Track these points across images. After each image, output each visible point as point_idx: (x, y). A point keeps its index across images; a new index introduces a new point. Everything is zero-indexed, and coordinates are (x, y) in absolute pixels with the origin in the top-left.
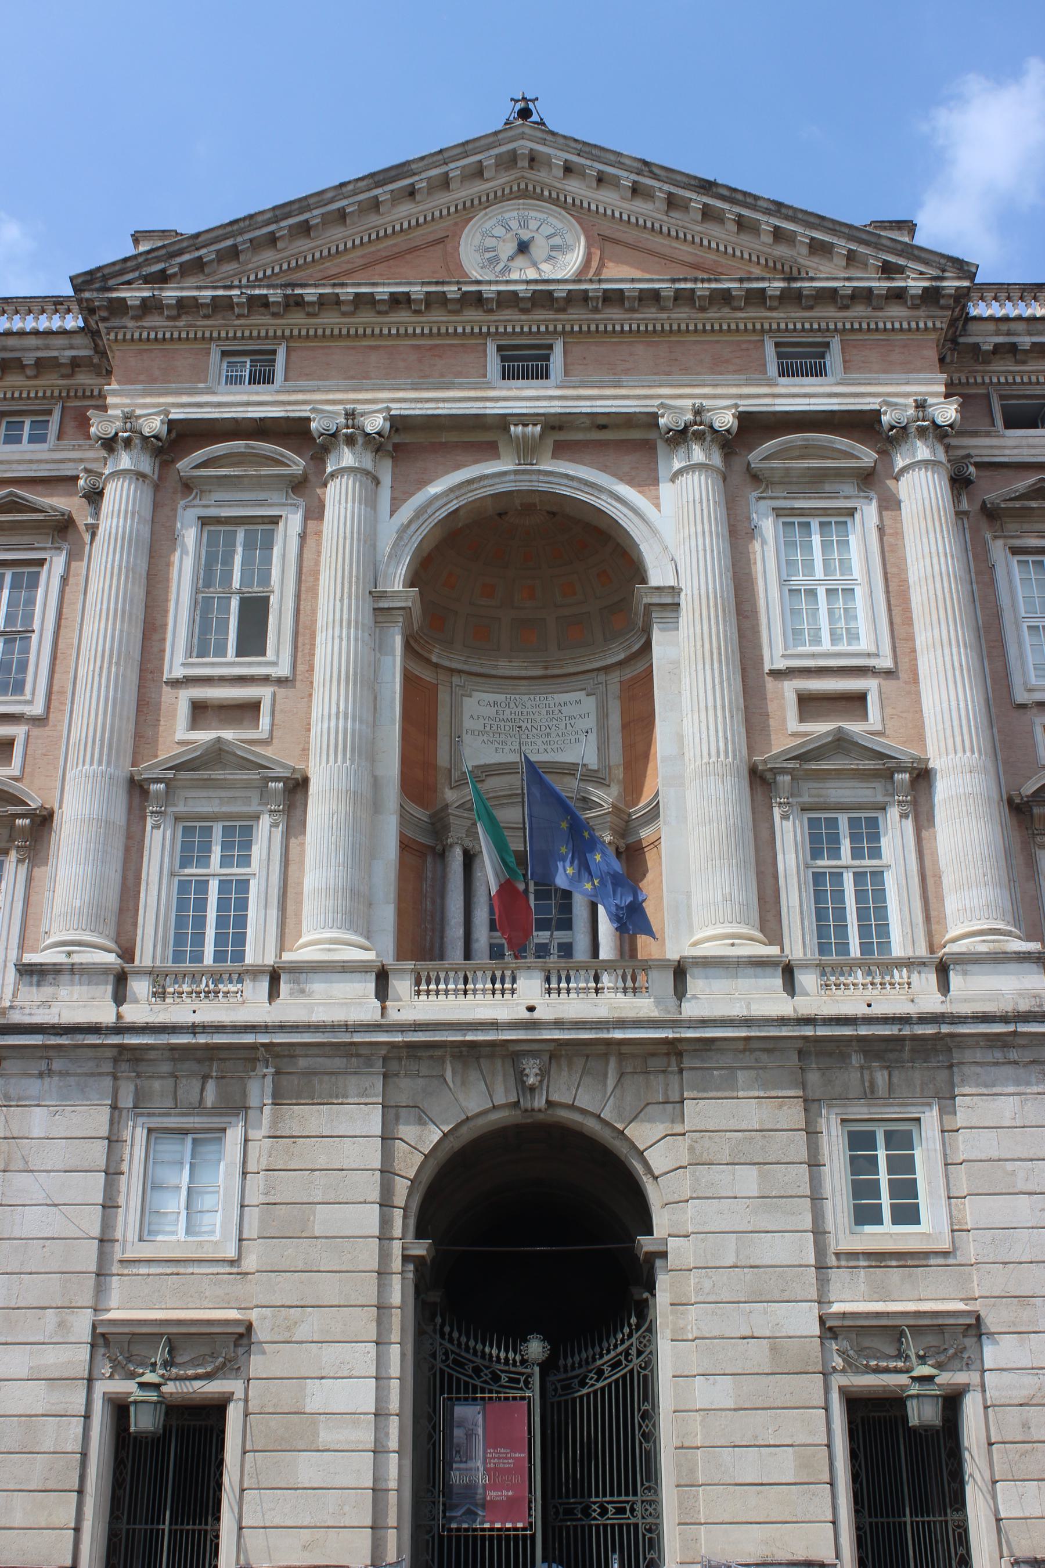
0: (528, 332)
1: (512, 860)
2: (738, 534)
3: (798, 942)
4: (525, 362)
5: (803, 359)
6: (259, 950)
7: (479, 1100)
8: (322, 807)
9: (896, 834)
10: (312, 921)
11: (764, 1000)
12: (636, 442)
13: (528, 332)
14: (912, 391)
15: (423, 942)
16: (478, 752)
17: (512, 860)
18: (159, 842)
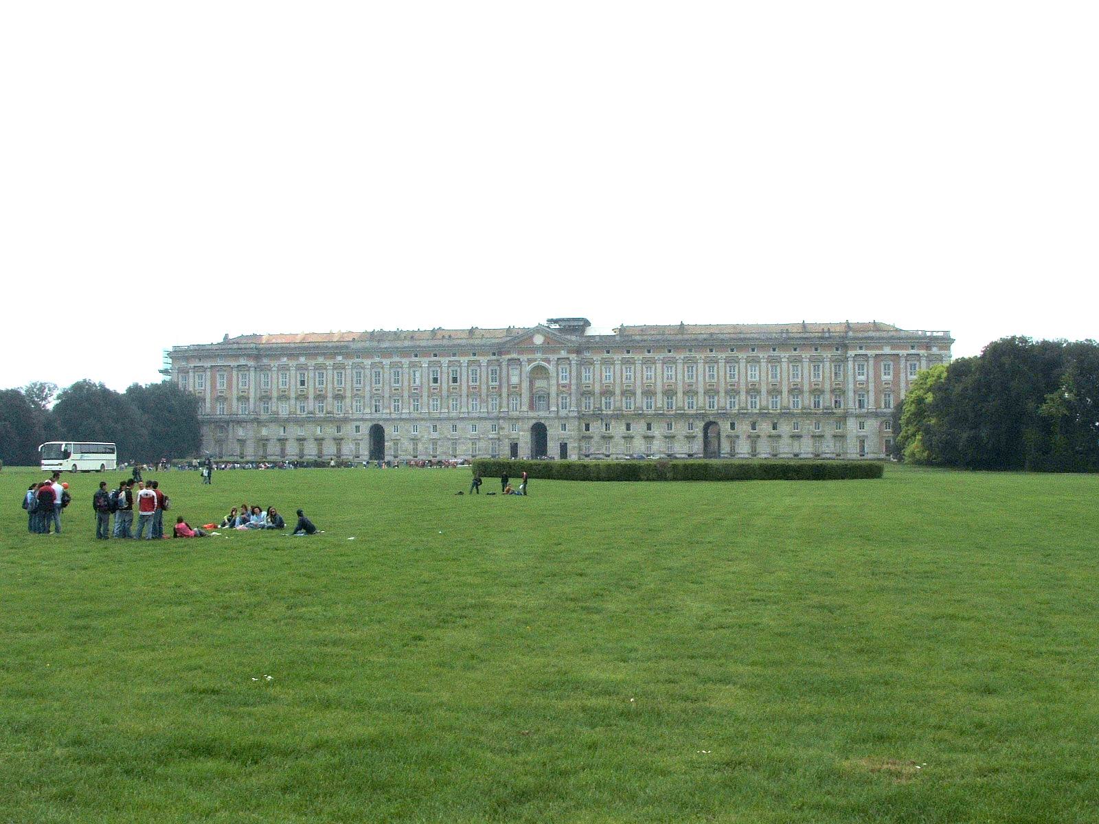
7: (534, 421)
12: (548, 361)
17: (537, 399)
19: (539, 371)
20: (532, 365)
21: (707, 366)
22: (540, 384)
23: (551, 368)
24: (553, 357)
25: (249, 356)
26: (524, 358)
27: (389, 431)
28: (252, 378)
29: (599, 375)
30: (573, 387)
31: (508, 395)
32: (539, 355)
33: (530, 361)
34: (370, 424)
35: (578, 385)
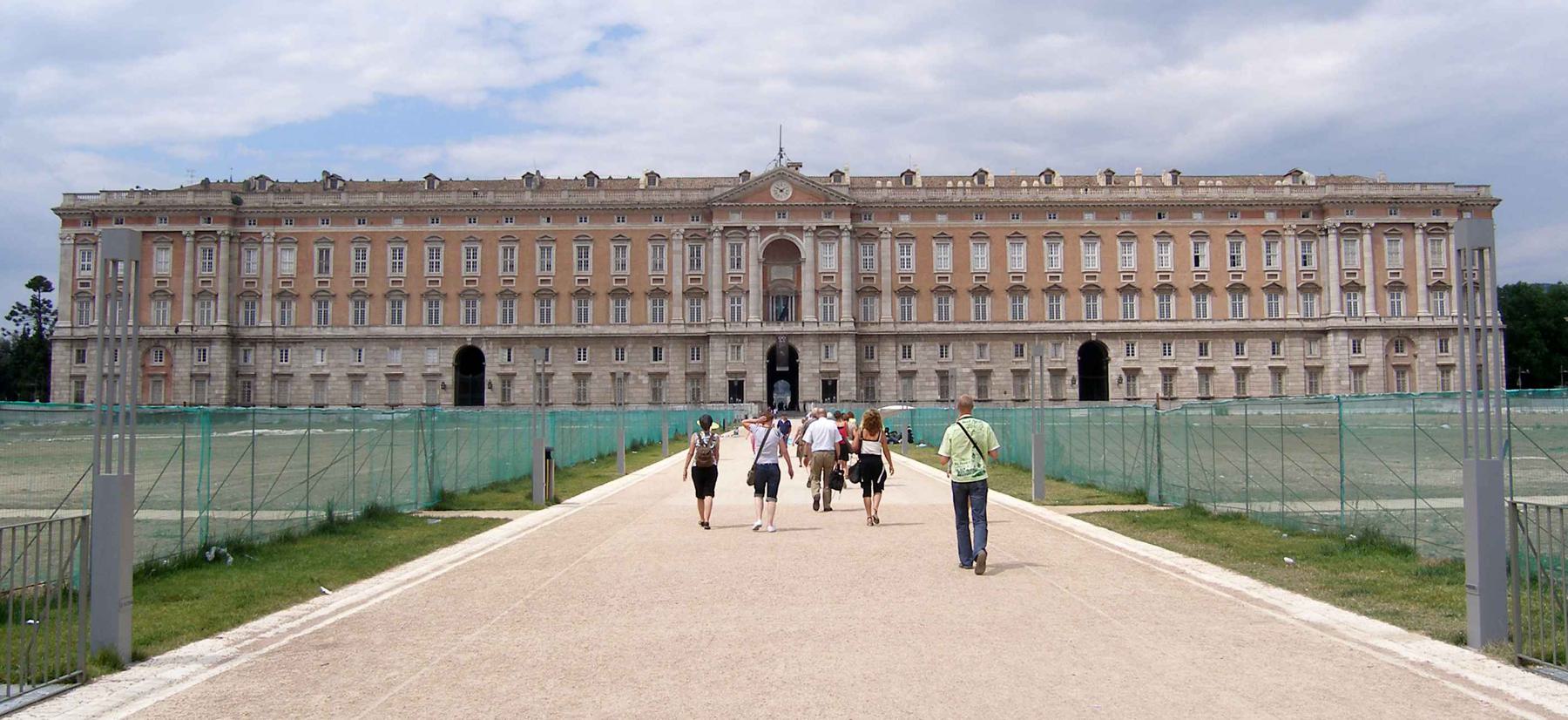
0: (782, 209)
1: (781, 304)
2: (816, 248)
3: (821, 318)
4: (782, 215)
5: (828, 214)
6: (743, 319)
8: (751, 297)
9: (836, 300)
10: (752, 317)
11: (815, 328)
12: (799, 230)
13: (782, 209)
14: (845, 223)
15: (766, 319)
16: (774, 277)
17: (781, 304)
18: (728, 300)
19: (782, 252)
20: (769, 238)
21: (897, 244)
22: (781, 272)
23: (805, 244)
24: (812, 224)
25: (220, 220)
26: (754, 224)
27: (494, 363)
28: (224, 256)
29: (891, 259)
30: (846, 278)
31: (816, 291)
32: (782, 222)
33: (764, 230)
34: (453, 349)
35: (855, 274)
